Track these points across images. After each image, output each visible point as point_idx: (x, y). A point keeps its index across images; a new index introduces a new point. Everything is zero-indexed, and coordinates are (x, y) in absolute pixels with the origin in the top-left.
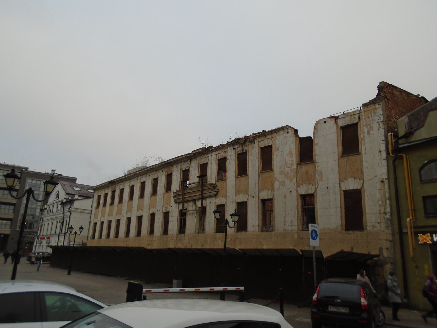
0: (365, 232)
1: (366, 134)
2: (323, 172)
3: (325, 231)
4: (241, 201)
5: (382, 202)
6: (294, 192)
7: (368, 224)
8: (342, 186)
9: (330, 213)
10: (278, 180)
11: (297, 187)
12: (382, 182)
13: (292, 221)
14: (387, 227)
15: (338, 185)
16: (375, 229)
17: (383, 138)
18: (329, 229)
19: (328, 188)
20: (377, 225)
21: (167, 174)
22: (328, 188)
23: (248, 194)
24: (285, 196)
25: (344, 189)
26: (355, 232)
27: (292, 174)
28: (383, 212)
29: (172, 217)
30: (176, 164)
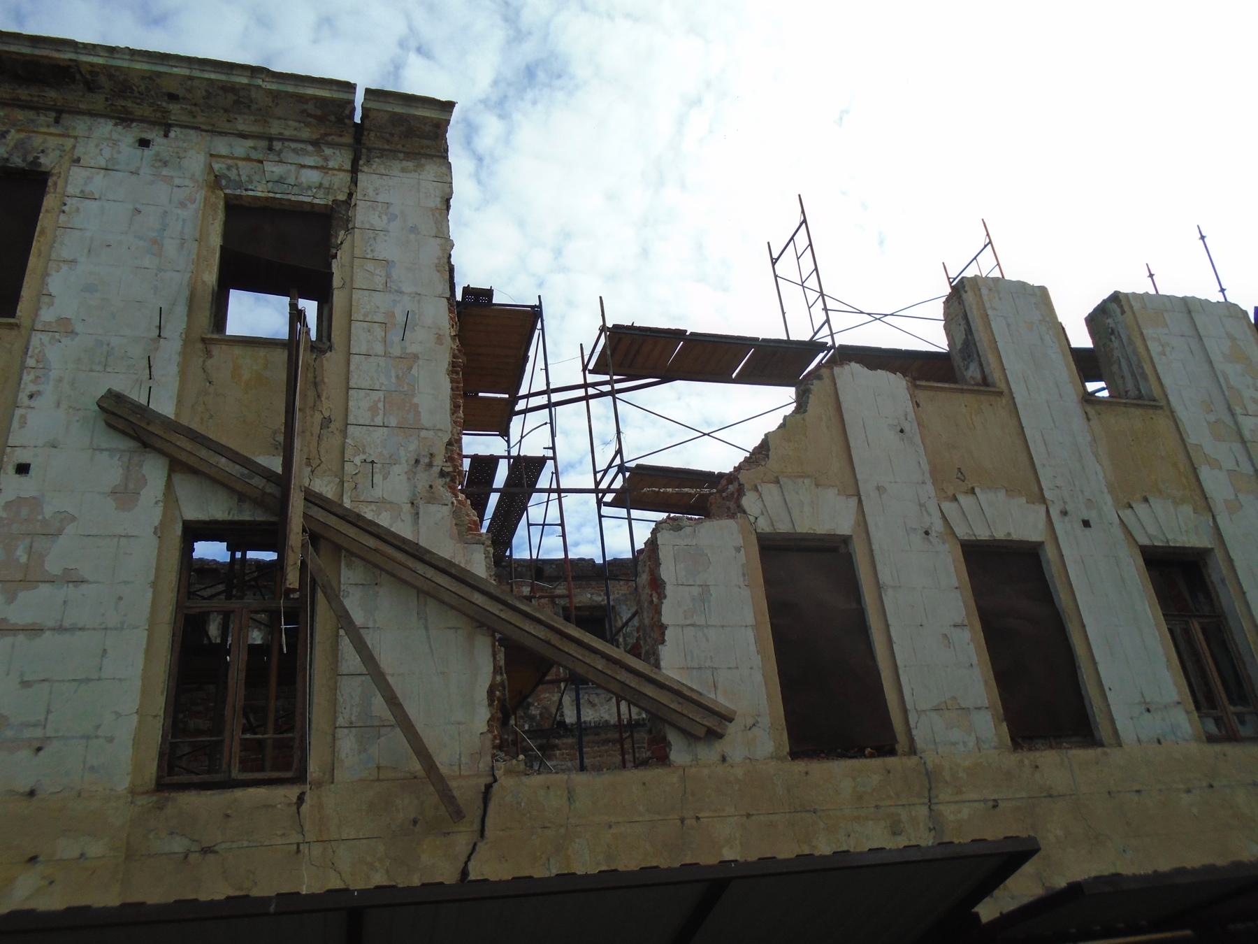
4: (1000, 535)
10: (1215, 464)
23: (1043, 500)
30: (124, 119)
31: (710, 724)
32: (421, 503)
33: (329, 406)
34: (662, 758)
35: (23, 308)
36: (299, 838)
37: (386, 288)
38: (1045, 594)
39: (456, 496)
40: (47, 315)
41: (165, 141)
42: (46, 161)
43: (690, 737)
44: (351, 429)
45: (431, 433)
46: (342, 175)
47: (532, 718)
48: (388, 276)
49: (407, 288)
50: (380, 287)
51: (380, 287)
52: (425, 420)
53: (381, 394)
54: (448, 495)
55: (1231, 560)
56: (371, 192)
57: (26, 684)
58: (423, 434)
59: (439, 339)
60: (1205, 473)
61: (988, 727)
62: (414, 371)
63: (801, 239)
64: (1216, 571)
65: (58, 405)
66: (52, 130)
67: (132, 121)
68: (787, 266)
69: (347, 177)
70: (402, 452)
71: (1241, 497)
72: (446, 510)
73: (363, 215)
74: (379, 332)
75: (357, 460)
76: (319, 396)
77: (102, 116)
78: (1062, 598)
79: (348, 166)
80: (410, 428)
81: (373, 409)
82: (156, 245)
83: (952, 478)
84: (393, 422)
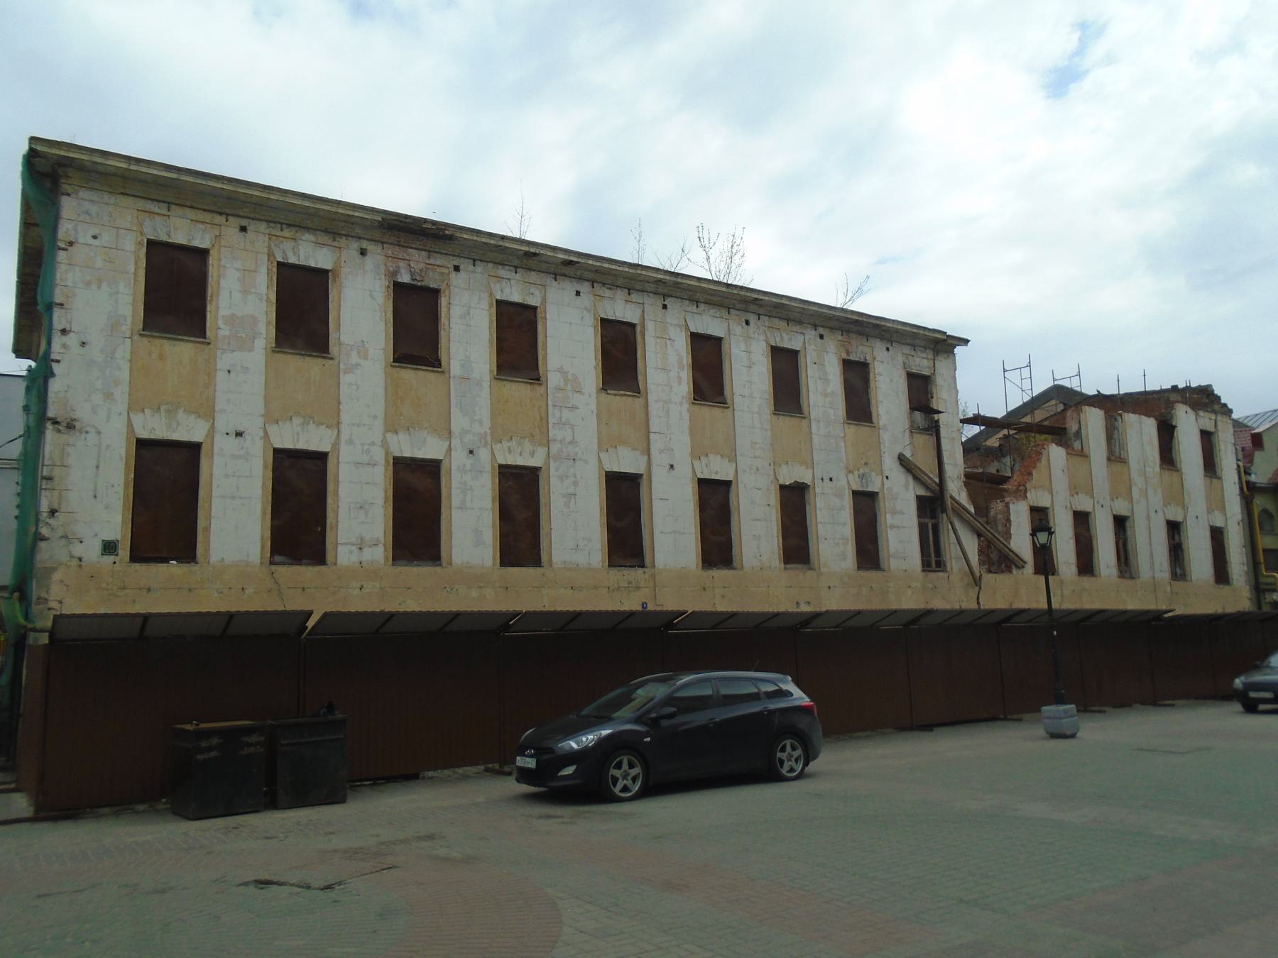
21: (845, 356)
24: (1148, 518)
29: (894, 513)
30: (882, 338)
31: (1020, 564)
34: (1010, 572)
35: (875, 419)
38: (1088, 529)
40: (881, 423)
42: (869, 360)
43: (1018, 567)
60: (1134, 489)
61: (1074, 569)
63: (1026, 372)
64: (1128, 524)
68: (1014, 376)
78: (1092, 531)
80: (955, 465)
83: (1074, 489)
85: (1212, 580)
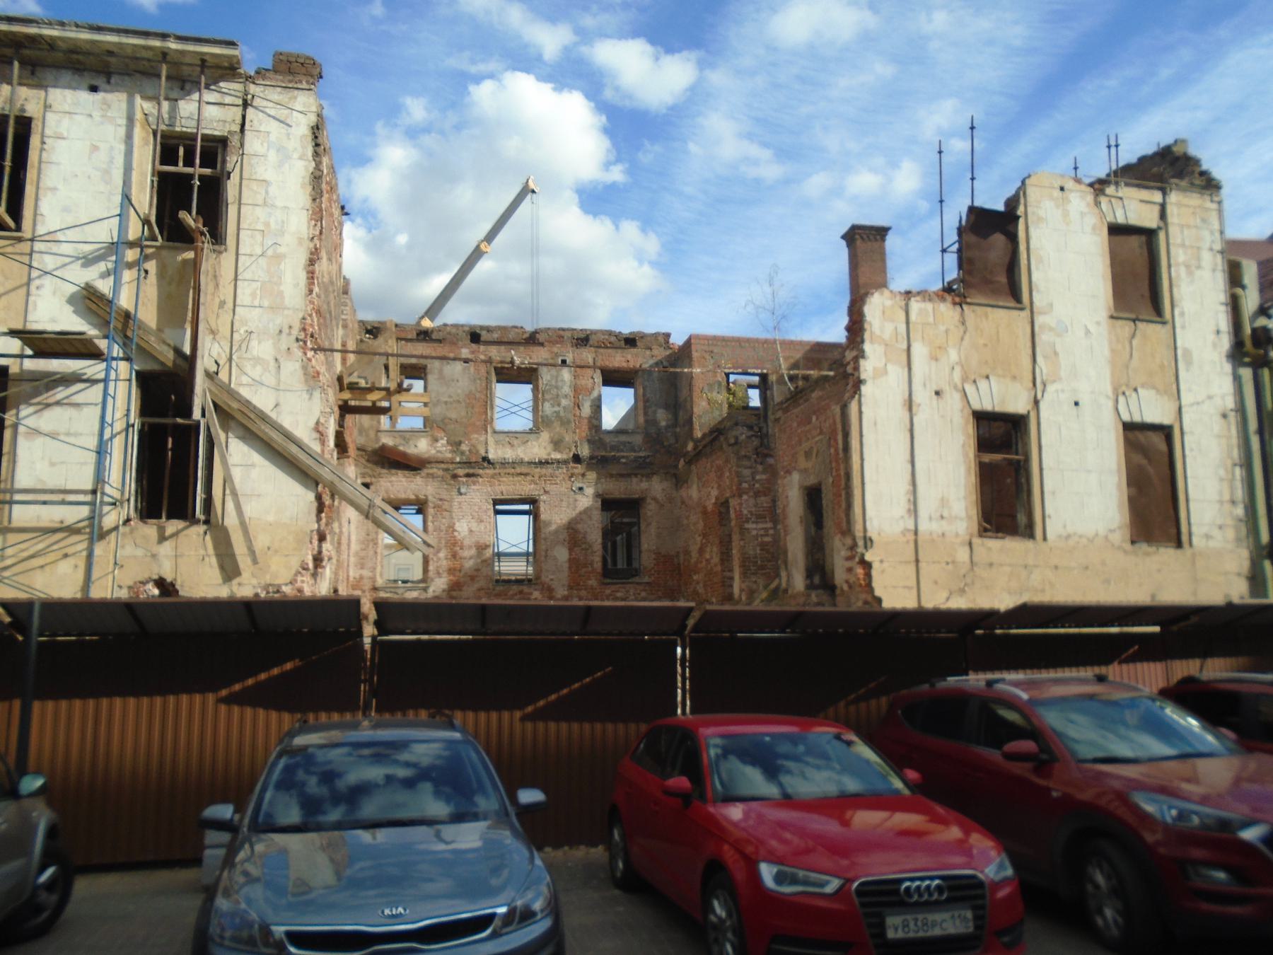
0: (1187, 551)
1: (1183, 270)
2: (1058, 349)
3: (1071, 542)
5: (1226, 470)
6: (953, 401)
7: (1194, 529)
8: (1122, 407)
9: (1080, 486)
11: (965, 379)
12: (1224, 416)
13: (944, 502)
14: (1238, 540)
15: (1110, 404)
16: (1212, 544)
17: (1222, 297)
18: (1081, 537)
19: (1076, 404)
20: (1216, 533)
22: (1076, 404)
24: (910, 404)
25: (1126, 417)
26: (1162, 550)
27: (942, 328)
28: (1227, 497)
32: (281, 360)
33: (226, 292)
36: (202, 552)
37: (265, 204)
39: (305, 354)
41: (108, 87)
44: (237, 309)
45: (290, 312)
46: (235, 109)
47: (463, 453)
48: (267, 192)
49: (279, 203)
50: (260, 202)
51: (260, 202)
52: (287, 302)
53: (259, 284)
54: (299, 353)
55: (860, 412)
56: (255, 122)
57: (52, 464)
58: (286, 312)
59: (300, 240)
62: (282, 267)
65: (54, 293)
66: (30, 82)
67: (84, 70)
69: (239, 111)
70: (271, 325)
71: (890, 367)
72: (298, 365)
73: (253, 144)
74: (259, 237)
75: (242, 331)
76: (217, 285)
77: (64, 67)
79: (240, 102)
81: (253, 295)
82: (107, 172)
84: (266, 304)
85: (1120, 536)
